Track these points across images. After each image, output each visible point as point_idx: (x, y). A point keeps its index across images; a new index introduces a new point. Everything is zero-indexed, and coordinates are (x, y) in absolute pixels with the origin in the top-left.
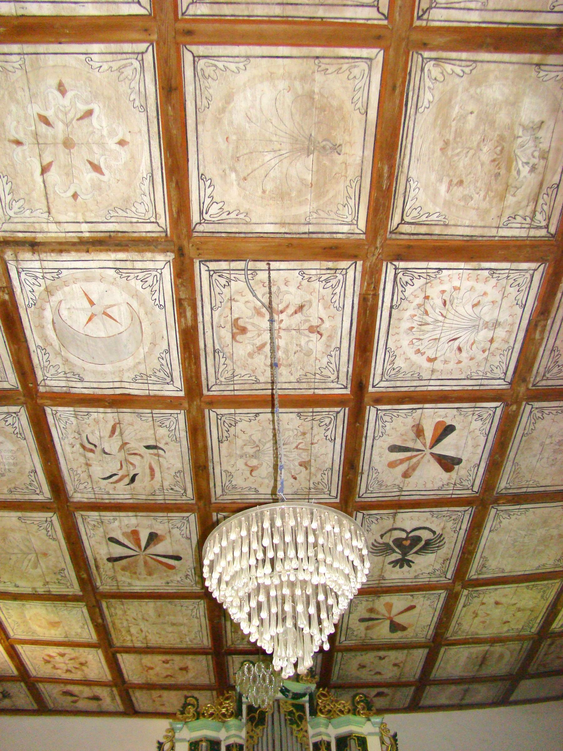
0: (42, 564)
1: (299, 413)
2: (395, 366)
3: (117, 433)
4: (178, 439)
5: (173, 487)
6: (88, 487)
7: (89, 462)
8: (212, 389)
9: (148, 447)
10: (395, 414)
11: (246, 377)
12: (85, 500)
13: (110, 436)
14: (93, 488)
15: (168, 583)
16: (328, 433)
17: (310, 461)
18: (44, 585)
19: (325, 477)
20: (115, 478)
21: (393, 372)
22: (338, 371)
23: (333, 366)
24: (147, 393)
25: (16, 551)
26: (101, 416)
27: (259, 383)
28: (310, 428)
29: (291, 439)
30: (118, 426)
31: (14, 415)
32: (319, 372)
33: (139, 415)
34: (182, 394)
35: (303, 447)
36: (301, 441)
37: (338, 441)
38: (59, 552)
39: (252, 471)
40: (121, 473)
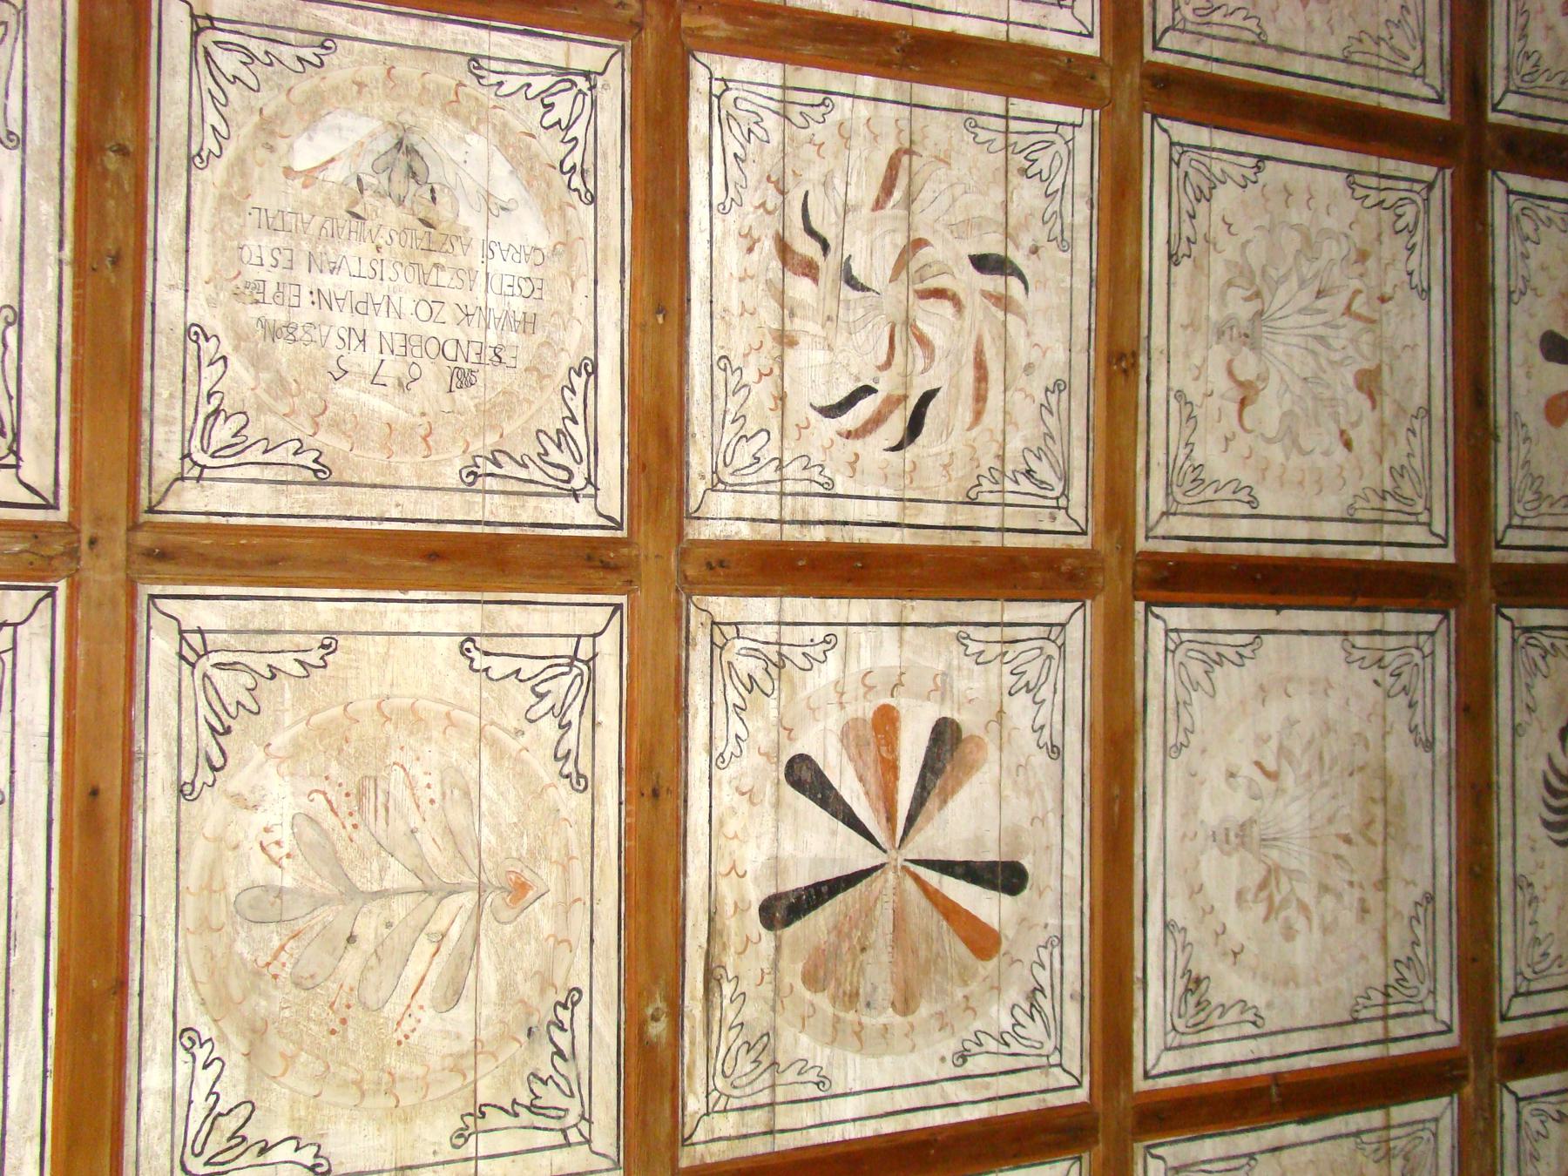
0: (490, 977)
1: (1351, 172)
2: (1530, 48)
3: (898, 195)
4: (1067, 234)
5: (1034, 465)
6: (766, 456)
7: (792, 326)
8: (1165, 43)
9: (981, 263)
10: (1542, 213)
11: (1237, 19)
12: (744, 532)
13: (878, 205)
14: (780, 468)
15: (963, 1056)
16: (1414, 263)
17: (1379, 367)
18: (462, 1135)
19: (1416, 442)
20: (866, 407)
21: (1527, 68)
22: (1423, 41)
23: (1411, 19)
24: (997, 32)
25: (397, 876)
26: (864, 109)
27: (1264, 44)
28: (1374, 235)
29: (1336, 270)
30: (905, 159)
31: (582, 83)
32: (1384, 34)
33: (972, 116)
34: (1091, 48)
35: (1364, 311)
36: (1356, 284)
37: (1437, 294)
38: (579, 870)
39: (1243, 403)
40: (886, 385)
